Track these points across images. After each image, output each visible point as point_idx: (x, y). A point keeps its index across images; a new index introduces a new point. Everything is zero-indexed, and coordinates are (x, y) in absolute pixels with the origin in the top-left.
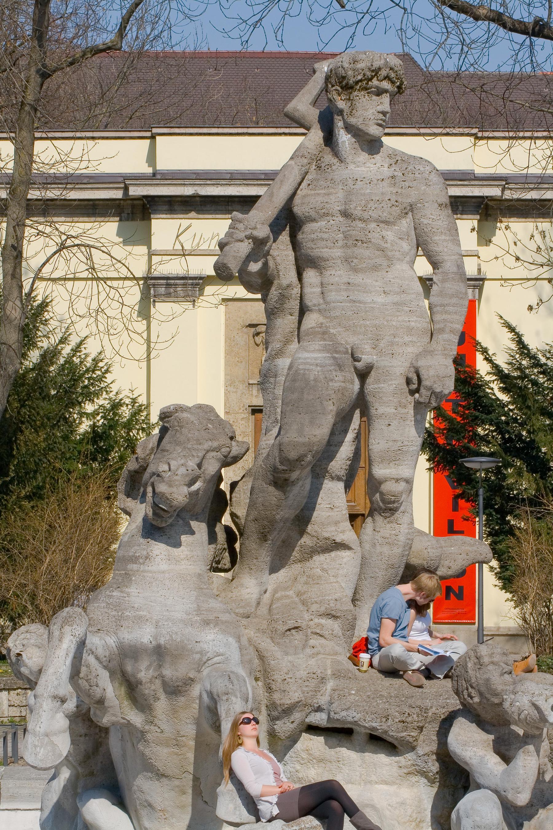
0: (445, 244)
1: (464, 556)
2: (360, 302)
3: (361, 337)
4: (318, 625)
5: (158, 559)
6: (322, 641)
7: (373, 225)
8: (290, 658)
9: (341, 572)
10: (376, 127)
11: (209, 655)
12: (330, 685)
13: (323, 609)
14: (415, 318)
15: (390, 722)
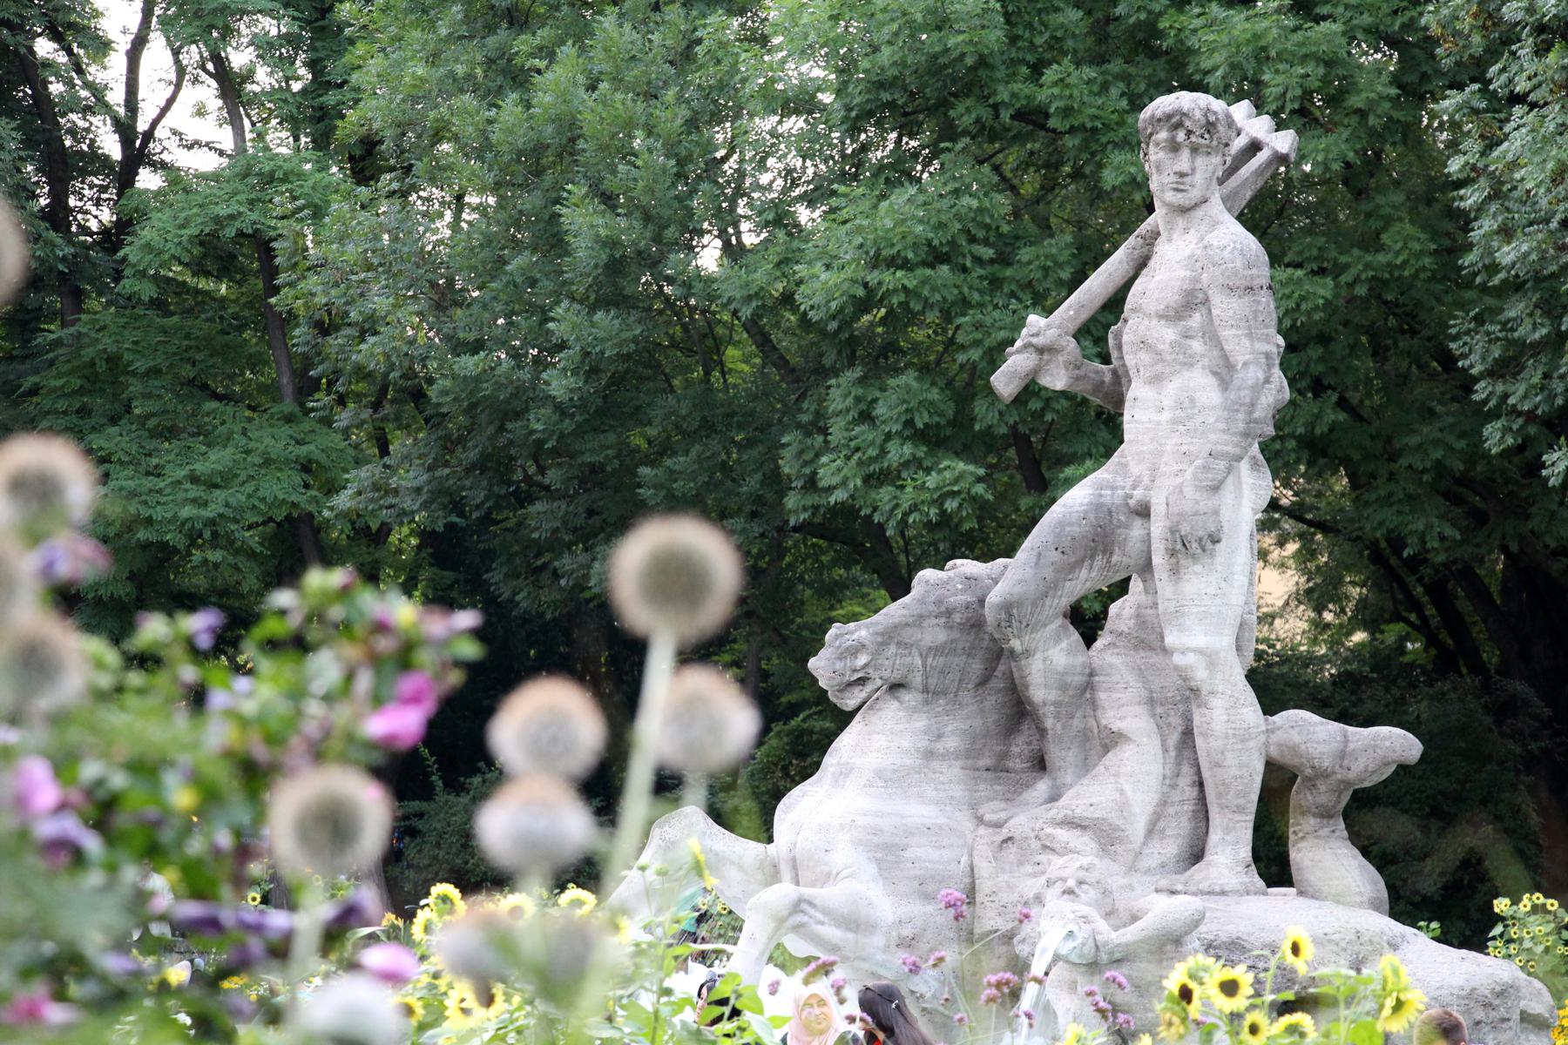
4: (1048, 836)
8: (1006, 877)
9: (1122, 770)
10: (1172, 193)
13: (1061, 816)
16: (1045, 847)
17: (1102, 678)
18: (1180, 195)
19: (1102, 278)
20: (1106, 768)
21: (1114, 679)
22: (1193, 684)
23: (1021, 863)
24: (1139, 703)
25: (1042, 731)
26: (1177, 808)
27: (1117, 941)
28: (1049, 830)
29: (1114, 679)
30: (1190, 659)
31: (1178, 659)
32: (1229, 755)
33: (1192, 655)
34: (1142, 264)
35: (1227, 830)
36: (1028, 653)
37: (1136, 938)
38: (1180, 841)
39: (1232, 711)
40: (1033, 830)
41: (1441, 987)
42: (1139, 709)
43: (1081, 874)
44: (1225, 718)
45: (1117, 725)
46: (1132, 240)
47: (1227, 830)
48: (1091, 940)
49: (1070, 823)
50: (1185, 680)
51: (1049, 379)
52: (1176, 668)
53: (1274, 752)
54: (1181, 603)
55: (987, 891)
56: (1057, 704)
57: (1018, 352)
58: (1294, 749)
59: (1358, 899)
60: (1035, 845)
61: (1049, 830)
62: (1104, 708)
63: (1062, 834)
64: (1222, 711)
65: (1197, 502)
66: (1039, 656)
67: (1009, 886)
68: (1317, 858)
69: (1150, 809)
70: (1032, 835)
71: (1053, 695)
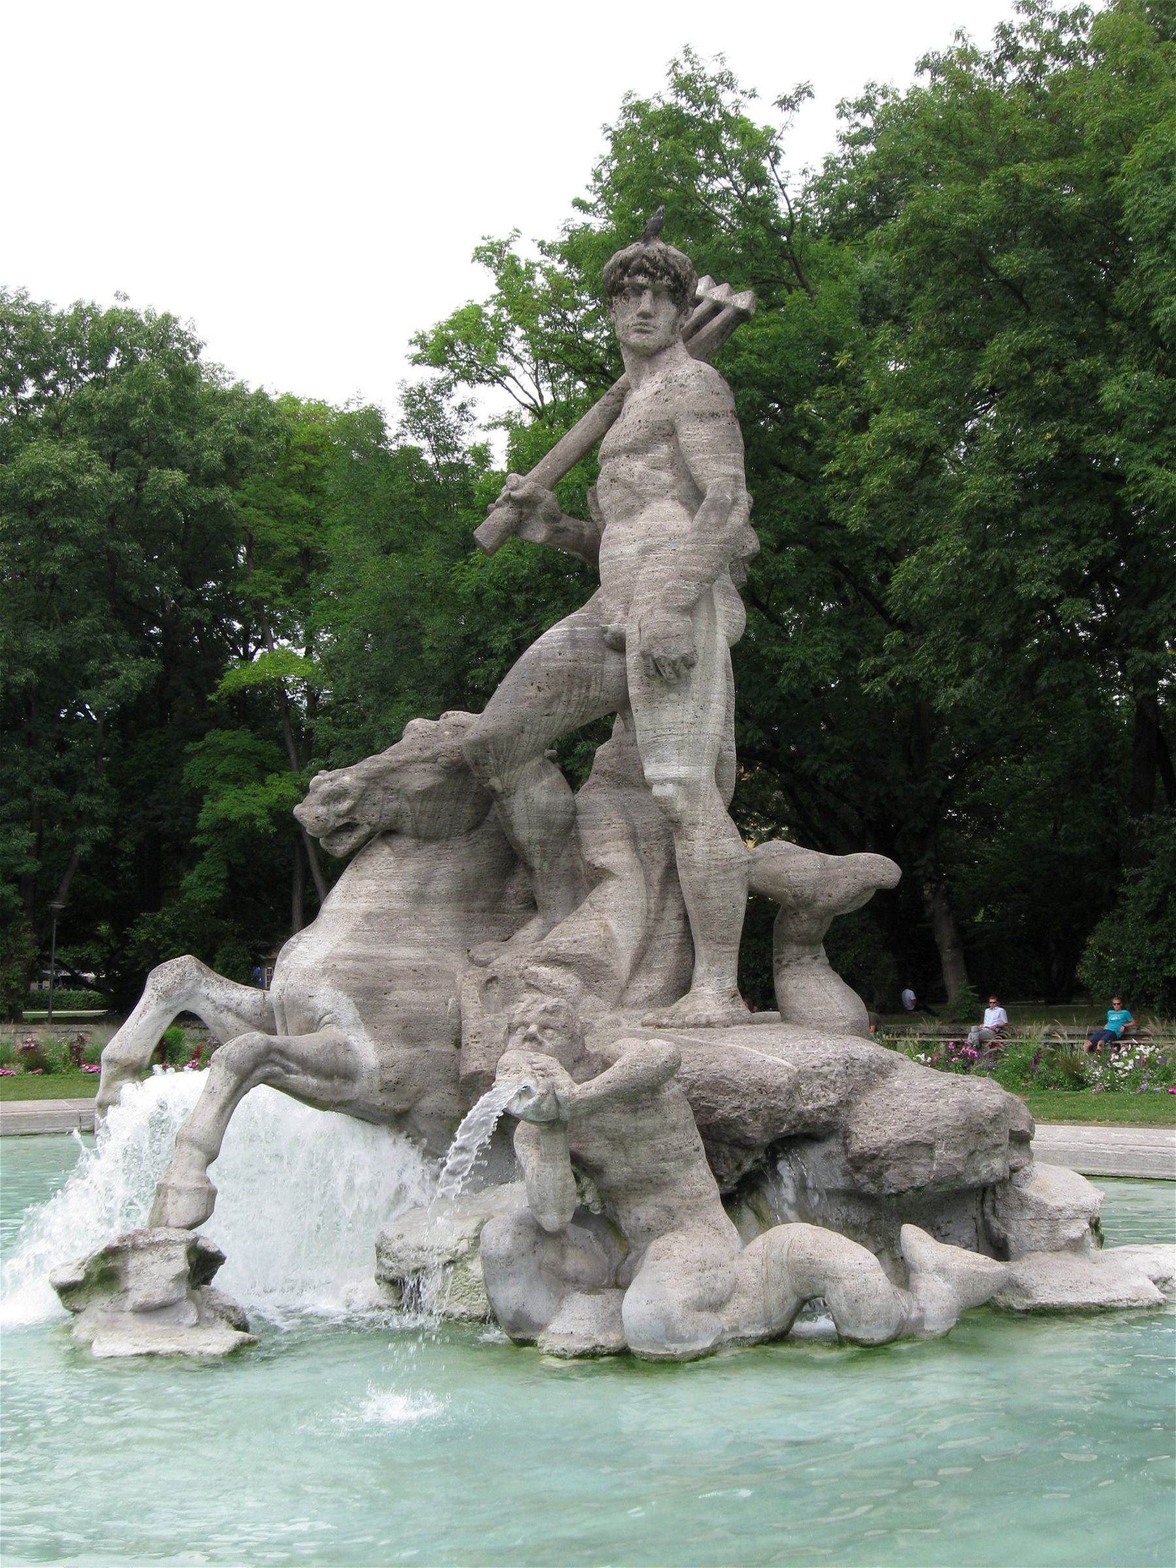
0: (703, 464)
1: (850, 880)
8: (492, 1017)
9: (606, 906)
10: (635, 335)
11: (320, 1013)
13: (544, 954)
14: (661, 567)
16: (529, 986)
17: (587, 817)
20: (592, 905)
22: (673, 815)
24: (621, 839)
25: (530, 870)
27: (579, 1097)
28: (533, 969)
30: (669, 790)
31: (657, 791)
32: (712, 886)
33: (670, 786)
35: (712, 962)
36: (509, 792)
38: (666, 974)
40: (517, 968)
41: (936, 1119)
42: (621, 844)
44: (707, 849)
45: (600, 861)
47: (712, 962)
49: (553, 960)
50: (665, 811)
52: (656, 799)
54: (659, 732)
55: (472, 1032)
56: (542, 843)
57: (498, 506)
59: (842, 1023)
61: (533, 969)
64: (701, 842)
65: (669, 624)
66: (520, 794)
67: (495, 1026)
70: (516, 973)
71: (536, 834)
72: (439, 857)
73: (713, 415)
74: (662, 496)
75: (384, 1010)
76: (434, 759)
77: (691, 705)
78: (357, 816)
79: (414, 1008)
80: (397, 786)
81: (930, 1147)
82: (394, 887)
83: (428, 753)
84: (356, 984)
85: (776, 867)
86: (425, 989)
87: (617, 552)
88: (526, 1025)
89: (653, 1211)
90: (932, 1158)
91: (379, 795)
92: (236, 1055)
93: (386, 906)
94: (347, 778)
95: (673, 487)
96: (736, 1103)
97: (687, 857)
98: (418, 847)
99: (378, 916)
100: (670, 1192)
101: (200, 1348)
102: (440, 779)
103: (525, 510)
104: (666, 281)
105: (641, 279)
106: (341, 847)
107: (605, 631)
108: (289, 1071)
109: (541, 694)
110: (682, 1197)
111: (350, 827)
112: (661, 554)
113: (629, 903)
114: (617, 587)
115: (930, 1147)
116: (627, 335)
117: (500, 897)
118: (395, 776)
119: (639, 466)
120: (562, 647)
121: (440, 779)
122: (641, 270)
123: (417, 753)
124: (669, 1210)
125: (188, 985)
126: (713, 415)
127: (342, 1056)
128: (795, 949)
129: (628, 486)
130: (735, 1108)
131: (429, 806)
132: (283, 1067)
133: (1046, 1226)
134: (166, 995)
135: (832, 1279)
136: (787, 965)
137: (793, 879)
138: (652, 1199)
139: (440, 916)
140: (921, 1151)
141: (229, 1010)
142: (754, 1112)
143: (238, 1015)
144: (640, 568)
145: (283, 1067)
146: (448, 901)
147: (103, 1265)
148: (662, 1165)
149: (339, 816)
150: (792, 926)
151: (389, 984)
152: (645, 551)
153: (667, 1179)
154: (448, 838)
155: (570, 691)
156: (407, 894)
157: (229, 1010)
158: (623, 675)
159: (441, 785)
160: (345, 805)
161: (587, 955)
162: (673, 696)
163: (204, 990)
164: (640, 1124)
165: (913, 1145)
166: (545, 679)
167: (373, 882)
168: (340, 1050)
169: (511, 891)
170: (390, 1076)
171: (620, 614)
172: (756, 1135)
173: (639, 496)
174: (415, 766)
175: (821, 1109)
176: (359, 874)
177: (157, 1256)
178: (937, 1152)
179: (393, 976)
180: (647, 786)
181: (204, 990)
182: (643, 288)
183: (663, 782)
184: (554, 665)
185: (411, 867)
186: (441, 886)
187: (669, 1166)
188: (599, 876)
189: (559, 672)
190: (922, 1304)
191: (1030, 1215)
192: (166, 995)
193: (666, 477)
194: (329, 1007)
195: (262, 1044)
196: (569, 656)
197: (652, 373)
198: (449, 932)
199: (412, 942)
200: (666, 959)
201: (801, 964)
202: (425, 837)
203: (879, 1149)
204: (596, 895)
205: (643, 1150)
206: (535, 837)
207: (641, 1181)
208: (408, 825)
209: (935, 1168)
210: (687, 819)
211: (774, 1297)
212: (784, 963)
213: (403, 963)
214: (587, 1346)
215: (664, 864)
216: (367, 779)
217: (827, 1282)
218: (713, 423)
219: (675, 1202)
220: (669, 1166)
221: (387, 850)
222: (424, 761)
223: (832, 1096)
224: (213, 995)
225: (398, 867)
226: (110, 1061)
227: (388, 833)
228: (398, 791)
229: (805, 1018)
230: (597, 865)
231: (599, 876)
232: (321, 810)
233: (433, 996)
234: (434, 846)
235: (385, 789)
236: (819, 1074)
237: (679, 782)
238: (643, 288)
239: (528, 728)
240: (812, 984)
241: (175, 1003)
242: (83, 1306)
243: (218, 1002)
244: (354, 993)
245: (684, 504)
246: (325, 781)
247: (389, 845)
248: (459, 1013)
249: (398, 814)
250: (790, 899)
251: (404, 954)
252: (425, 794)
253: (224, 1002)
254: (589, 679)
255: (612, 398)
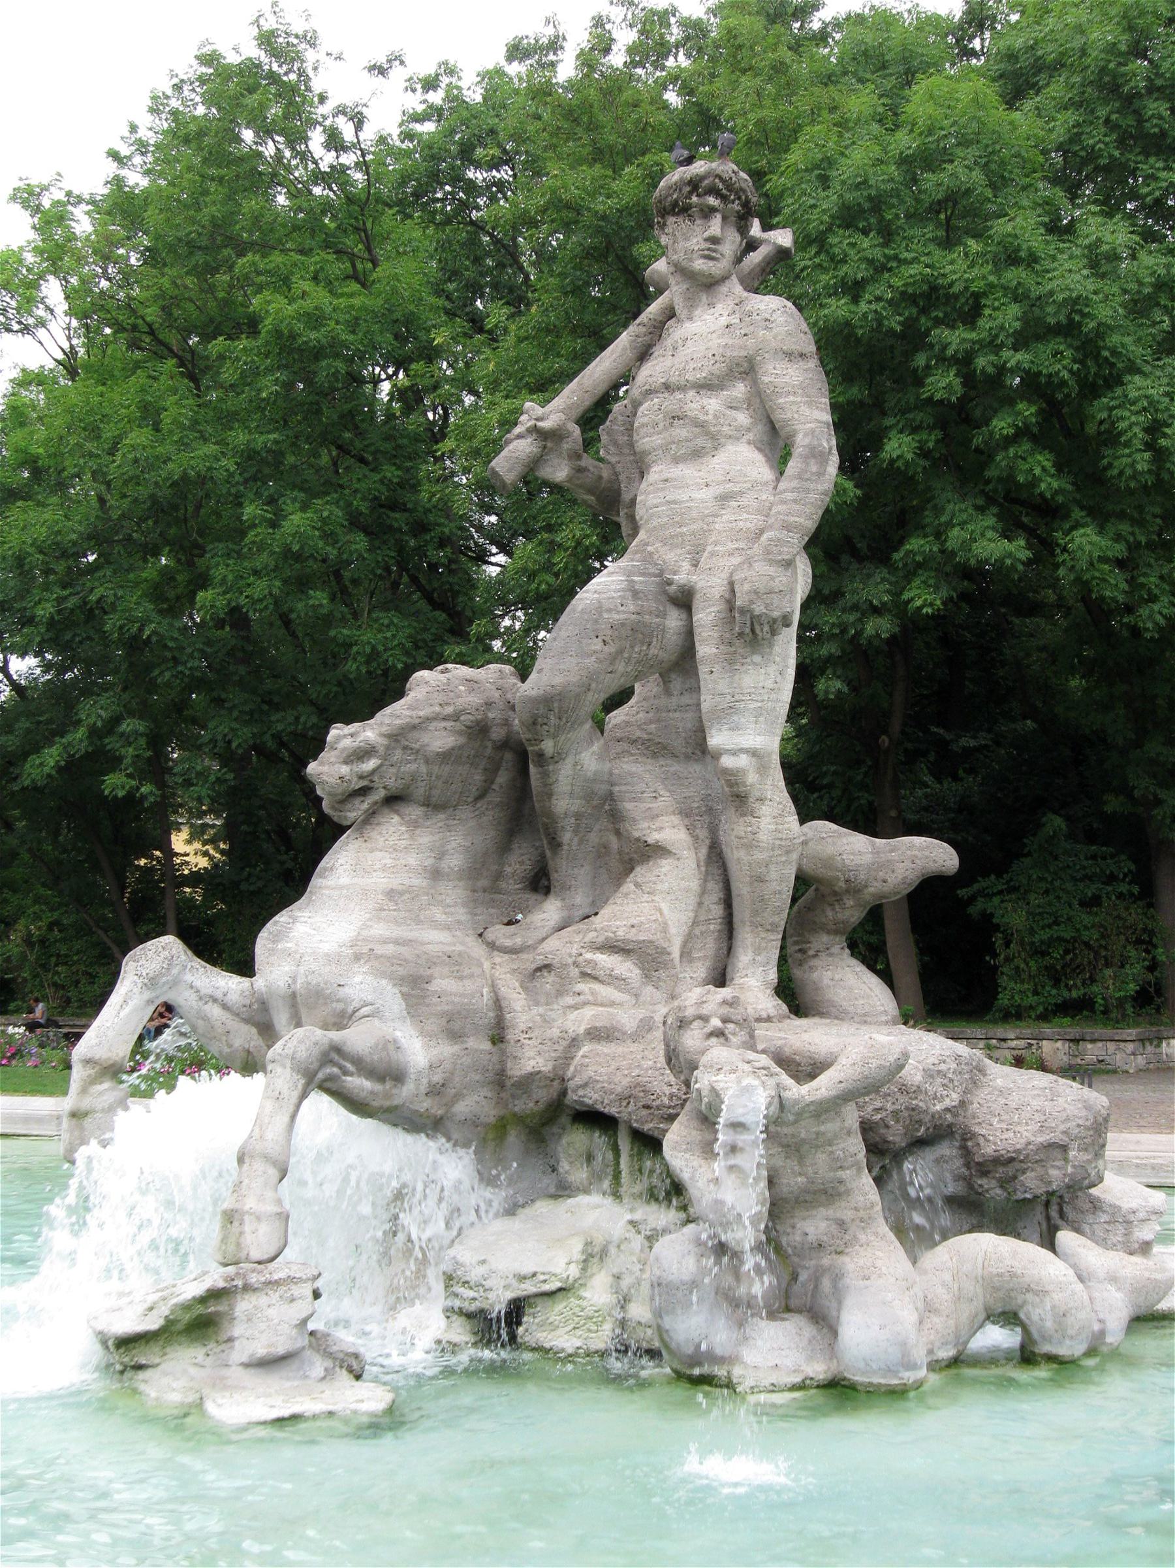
0: (794, 408)
1: (908, 864)
2: (675, 502)
3: (679, 551)
4: (589, 962)
5: (340, 871)
6: (596, 986)
7: (691, 393)
8: (541, 1010)
9: (659, 887)
10: (701, 261)
11: (355, 1004)
12: (585, 1049)
13: (601, 939)
14: (745, 516)
15: (631, 1107)
16: (584, 975)
17: (623, 788)
18: (711, 263)
19: (619, 350)
20: (637, 885)
21: (638, 788)
22: (742, 789)
23: (560, 993)
24: (673, 813)
25: (555, 845)
26: (704, 928)
27: (808, 1099)
28: (589, 956)
29: (638, 788)
30: (743, 761)
31: (727, 761)
32: (773, 867)
33: (744, 756)
34: (643, 355)
35: (758, 951)
36: (558, 757)
37: (833, 1093)
38: (708, 963)
39: (779, 820)
40: (570, 956)
41: (1067, 1119)
42: (676, 819)
43: (725, 1010)
44: (773, 827)
45: (653, 837)
46: (633, 328)
47: (758, 951)
48: (776, 1100)
49: (613, 947)
50: (730, 784)
51: (548, 470)
52: (726, 771)
53: (809, 868)
54: (737, 697)
55: (522, 1027)
56: (578, 816)
57: (519, 437)
58: (828, 862)
59: (884, 1018)
60: (574, 972)
61: (589, 956)
62: (634, 820)
63: (605, 960)
64: (768, 819)
65: (772, 578)
66: (570, 761)
67: (545, 1021)
68: (837, 977)
69: (685, 929)
70: (570, 961)
71: (576, 805)
72: (449, 828)
73: (802, 355)
74: (738, 439)
75: (427, 1001)
76: (455, 717)
77: (772, 669)
78: (376, 778)
79: (457, 1000)
80: (417, 746)
81: (1064, 1148)
82: (412, 860)
83: (449, 710)
84: (401, 971)
85: (828, 849)
86: (461, 978)
87: (685, 497)
88: (705, 1019)
89: (823, 1225)
90: (1066, 1160)
91: (398, 755)
92: (302, 1054)
93: (407, 882)
94: (369, 732)
95: (749, 430)
96: (878, 1104)
97: (751, 836)
98: (427, 817)
99: (401, 893)
100: (843, 1204)
101: (354, 1406)
102: (462, 740)
103: (549, 445)
104: (736, 206)
105: (712, 201)
106: (355, 811)
107: (670, 583)
108: (346, 1073)
109: (607, 649)
110: (857, 1209)
111: (363, 792)
112: (744, 501)
113: (684, 884)
114: (682, 535)
115: (1064, 1148)
116: (691, 260)
117: (498, 876)
118: (416, 734)
119: (713, 404)
120: (623, 597)
121: (462, 740)
122: (713, 191)
123: (437, 709)
124: (841, 1224)
125: (175, 971)
126: (802, 355)
127: (394, 1056)
128: (825, 938)
129: (701, 425)
130: (878, 1110)
131: (447, 769)
132: (341, 1067)
133: (1121, 1230)
134: (152, 983)
135: (1036, 1293)
136: (816, 956)
137: (847, 862)
138: (822, 1211)
139: (454, 893)
140: (1057, 1154)
141: (215, 1000)
142: (895, 1114)
143: (225, 1007)
144: (716, 516)
145: (341, 1067)
146: (460, 879)
147: (200, 1310)
148: (840, 1173)
149: (361, 777)
150: (830, 913)
151: (429, 972)
152: (724, 498)
153: (843, 1189)
154: (455, 807)
155: (632, 647)
156: (425, 868)
157: (215, 1000)
158: (689, 633)
159: (461, 747)
160: (371, 764)
161: (651, 942)
162: (757, 658)
163: (188, 977)
164: (822, 1128)
165: (1050, 1146)
166: (609, 632)
167: (387, 855)
168: (391, 1047)
169: (508, 870)
170: (437, 1078)
171: (686, 566)
172: (897, 1139)
173: (713, 437)
174: (434, 724)
175: (947, 1110)
176: (368, 845)
177: (274, 1296)
178: (1072, 1154)
179: (432, 963)
180: (716, 756)
181: (188, 977)
182: (713, 210)
183: (735, 753)
184: (616, 616)
185: (426, 838)
186: (454, 861)
187: (846, 1174)
188: (651, 852)
189: (623, 625)
190: (1101, 1316)
191: (1104, 1217)
192: (152, 983)
193: (743, 418)
194: (370, 998)
195: (326, 1041)
196: (632, 608)
197: (711, 305)
198: (461, 914)
199: (435, 924)
200: (708, 947)
201: (831, 955)
202: (433, 805)
203: (1018, 1151)
204: (641, 873)
205: (821, 1158)
206: (574, 808)
207: (815, 1193)
208: (420, 791)
209: (1070, 1170)
210: (756, 794)
211: (966, 1315)
212: (811, 953)
213: (438, 948)
214: (797, 1379)
215: (708, 842)
216: (389, 736)
217: (1029, 1297)
218: (802, 364)
219: (847, 1215)
220: (846, 1174)
221: (396, 819)
222: (444, 719)
223: (954, 1096)
224: (198, 984)
225: (412, 838)
226: (88, 1062)
227: (393, 800)
228: (418, 751)
229: (846, 1012)
230: (650, 840)
231: (651, 852)
232: (345, 770)
233: (469, 986)
234: (442, 816)
235: (405, 748)
236: (939, 1072)
237: (754, 753)
238: (713, 210)
239: (594, 685)
240: (850, 976)
241: (158, 992)
242: (157, 1361)
243: (203, 991)
244: (399, 981)
245: (760, 450)
246: (345, 736)
247: (397, 812)
248: (498, 1004)
249: (414, 778)
250: (842, 884)
251: (436, 939)
252: (445, 757)
253: (209, 991)
254: (651, 635)
255: (643, 330)
